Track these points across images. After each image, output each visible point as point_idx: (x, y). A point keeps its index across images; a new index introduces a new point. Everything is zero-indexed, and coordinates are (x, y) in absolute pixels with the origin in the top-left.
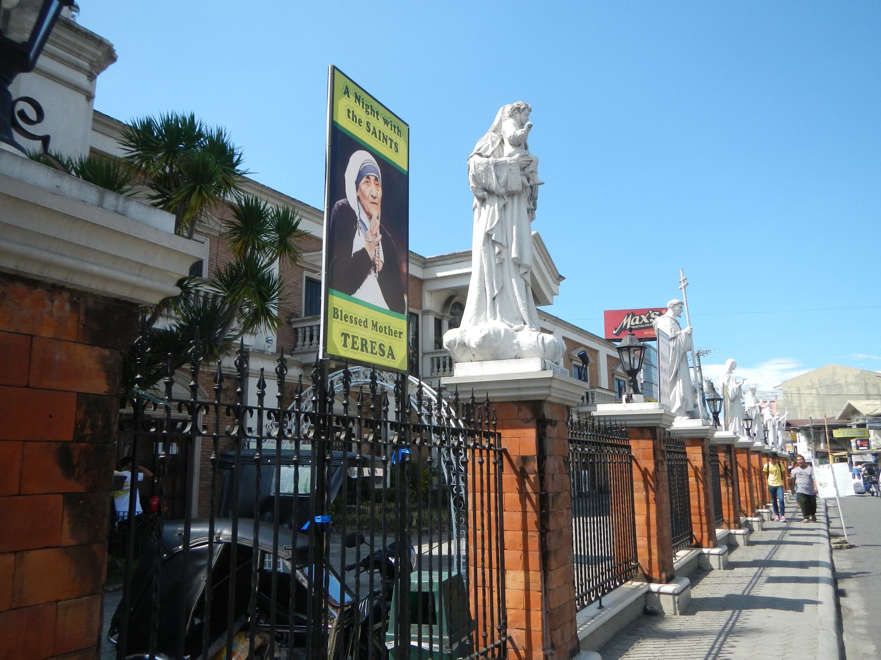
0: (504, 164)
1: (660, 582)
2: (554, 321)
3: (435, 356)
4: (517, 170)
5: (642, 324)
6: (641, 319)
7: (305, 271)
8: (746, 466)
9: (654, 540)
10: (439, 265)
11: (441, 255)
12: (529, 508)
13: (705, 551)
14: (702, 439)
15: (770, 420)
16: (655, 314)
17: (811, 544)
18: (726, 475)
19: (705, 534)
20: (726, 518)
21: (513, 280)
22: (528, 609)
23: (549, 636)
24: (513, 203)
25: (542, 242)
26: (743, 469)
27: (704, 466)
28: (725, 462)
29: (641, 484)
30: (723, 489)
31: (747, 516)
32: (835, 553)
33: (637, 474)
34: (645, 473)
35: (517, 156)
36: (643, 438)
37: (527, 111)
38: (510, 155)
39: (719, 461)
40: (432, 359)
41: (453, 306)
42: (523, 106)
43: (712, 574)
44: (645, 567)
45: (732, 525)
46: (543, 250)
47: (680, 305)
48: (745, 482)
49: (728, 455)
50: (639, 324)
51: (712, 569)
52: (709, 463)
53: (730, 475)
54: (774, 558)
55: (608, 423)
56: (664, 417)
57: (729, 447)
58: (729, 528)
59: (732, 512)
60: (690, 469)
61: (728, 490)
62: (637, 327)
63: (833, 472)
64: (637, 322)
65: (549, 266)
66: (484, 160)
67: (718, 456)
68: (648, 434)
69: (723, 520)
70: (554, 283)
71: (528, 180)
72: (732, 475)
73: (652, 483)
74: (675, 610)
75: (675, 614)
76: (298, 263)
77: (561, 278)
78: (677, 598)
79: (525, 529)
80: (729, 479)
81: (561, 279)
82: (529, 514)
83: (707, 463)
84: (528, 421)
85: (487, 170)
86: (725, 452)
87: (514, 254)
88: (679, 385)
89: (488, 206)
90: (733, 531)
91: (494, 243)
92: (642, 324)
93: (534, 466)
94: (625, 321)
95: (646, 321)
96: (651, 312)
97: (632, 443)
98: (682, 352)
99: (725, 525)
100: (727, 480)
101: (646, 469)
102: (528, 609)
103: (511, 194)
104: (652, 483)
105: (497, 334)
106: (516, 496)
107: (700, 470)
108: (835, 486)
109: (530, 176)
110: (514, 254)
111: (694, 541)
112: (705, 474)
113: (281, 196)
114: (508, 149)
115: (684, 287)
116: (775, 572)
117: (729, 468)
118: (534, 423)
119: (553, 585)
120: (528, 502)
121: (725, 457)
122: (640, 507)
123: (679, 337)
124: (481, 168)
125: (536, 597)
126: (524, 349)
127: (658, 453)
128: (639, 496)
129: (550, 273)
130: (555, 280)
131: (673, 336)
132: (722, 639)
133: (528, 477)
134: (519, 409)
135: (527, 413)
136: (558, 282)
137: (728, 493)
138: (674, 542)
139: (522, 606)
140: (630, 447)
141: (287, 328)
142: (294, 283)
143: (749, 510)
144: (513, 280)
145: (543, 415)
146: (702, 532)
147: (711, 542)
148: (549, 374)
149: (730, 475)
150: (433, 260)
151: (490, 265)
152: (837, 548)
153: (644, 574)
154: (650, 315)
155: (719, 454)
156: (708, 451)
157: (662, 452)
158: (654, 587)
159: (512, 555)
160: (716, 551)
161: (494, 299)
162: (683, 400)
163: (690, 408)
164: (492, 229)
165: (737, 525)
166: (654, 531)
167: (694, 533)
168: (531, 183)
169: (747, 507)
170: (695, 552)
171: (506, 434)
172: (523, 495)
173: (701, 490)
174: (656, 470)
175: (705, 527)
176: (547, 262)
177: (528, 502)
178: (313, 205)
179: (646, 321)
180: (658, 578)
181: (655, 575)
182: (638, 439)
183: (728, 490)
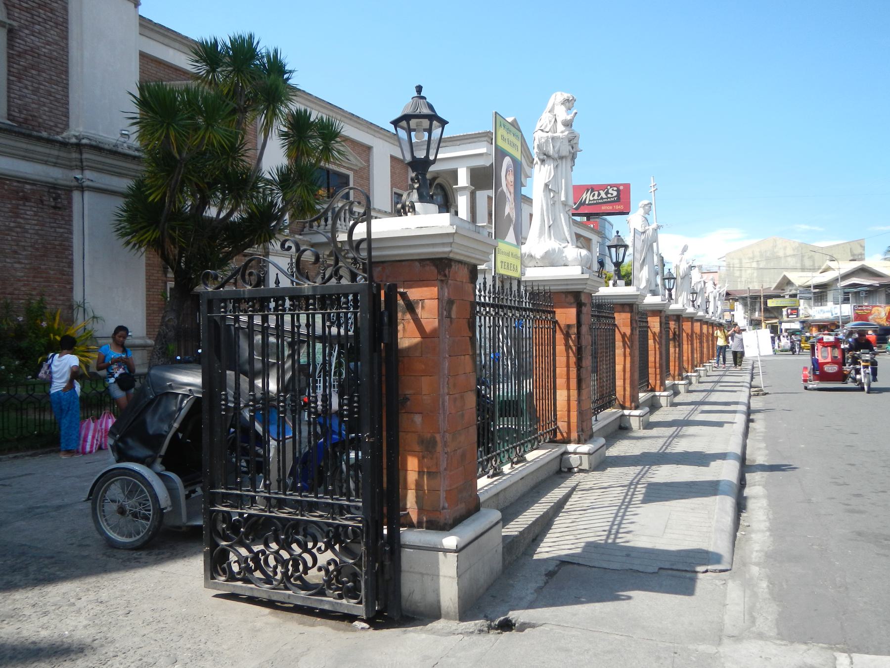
0: (558, 138)
1: (631, 409)
4: (566, 143)
5: (600, 199)
6: (599, 194)
8: (689, 332)
9: (628, 381)
12: (571, 354)
13: (657, 394)
14: (660, 311)
15: (712, 292)
16: (613, 190)
17: (735, 391)
18: (674, 339)
19: (658, 382)
20: (672, 372)
21: (562, 215)
22: (569, 411)
23: (580, 425)
24: (562, 163)
26: (688, 335)
27: (661, 332)
28: (674, 329)
29: (621, 344)
30: (672, 350)
31: (687, 372)
32: (752, 398)
33: (618, 337)
34: (624, 336)
35: (566, 133)
36: (624, 312)
37: (573, 101)
38: (562, 132)
39: (669, 328)
41: (435, 187)
42: (571, 98)
43: (662, 409)
44: (621, 399)
45: (677, 377)
47: (649, 205)
48: (688, 345)
50: (598, 200)
51: (662, 407)
52: (664, 329)
54: (707, 400)
55: (597, 301)
56: (639, 297)
57: (679, 317)
58: (674, 380)
59: (677, 368)
60: (650, 334)
61: (675, 351)
62: (595, 202)
64: (596, 197)
66: (545, 135)
67: (669, 324)
68: (628, 309)
69: (670, 374)
71: (573, 148)
73: (628, 343)
74: (640, 426)
75: (640, 429)
78: (641, 418)
79: (568, 366)
80: (676, 342)
82: (570, 358)
83: (663, 329)
84: (571, 304)
85: (547, 141)
86: (675, 321)
87: (563, 199)
88: (646, 268)
89: (546, 165)
90: (676, 382)
91: (550, 190)
92: (600, 199)
93: (575, 330)
94: (584, 196)
95: (604, 196)
96: (609, 187)
97: (616, 315)
98: (649, 244)
99: (671, 378)
101: (624, 333)
102: (569, 411)
103: (561, 158)
104: (628, 343)
105: (554, 250)
106: (563, 348)
109: (574, 146)
110: (563, 199)
111: (650, 387)
112: (660, 337)
114: (560, 127)
115: (654, 191)
116: (707, 408)
117: (677, 333)
118: (575, 305)
119: (583, 398)
120: (570, 351)
121: (675, 324)
122: (619, 359)
123: (647, 232)
124: (543, 140)
125: (574, 404)
126: (569, 260)
127: (634, 322)
128: (619, 351)
131: (643, 231)
132: (671, 439)
133: (571, 337)
134: (566, 297)
135: (571, 299)
137: (675, 353)
138: (640, 384)
139: (566, 409)
140: (615, 318)
144: (562, 215)
145: (581, 300)
146: (656, 380)
147: (662, 388)
148: (586, 276)
151: (547, 205)
153: (620, 404)
154: (608, 191)
155: (670, 323)
156: (663, 320)
157: (636, 321)
158: (626, 412)
159: (561, 381)
160: (665, 393)
161: (550, 227)
162: (648, 281)
163: (653, 287)
164: (549, 181)
165: (680, 377)
166: (628, 375)
167: (650, 381)
168: (574, 150)
170: (650, 394)
171: (558, 311)
172: (567, 347)
173: (657, 349)
174: (632, 334)
175: (658, 377)
177: (570, 351)
178: (314, 94)
179: (604, 196)
180: (629, 406)
181: (628, 404)
182: (620, 312)
183: (675, 351)
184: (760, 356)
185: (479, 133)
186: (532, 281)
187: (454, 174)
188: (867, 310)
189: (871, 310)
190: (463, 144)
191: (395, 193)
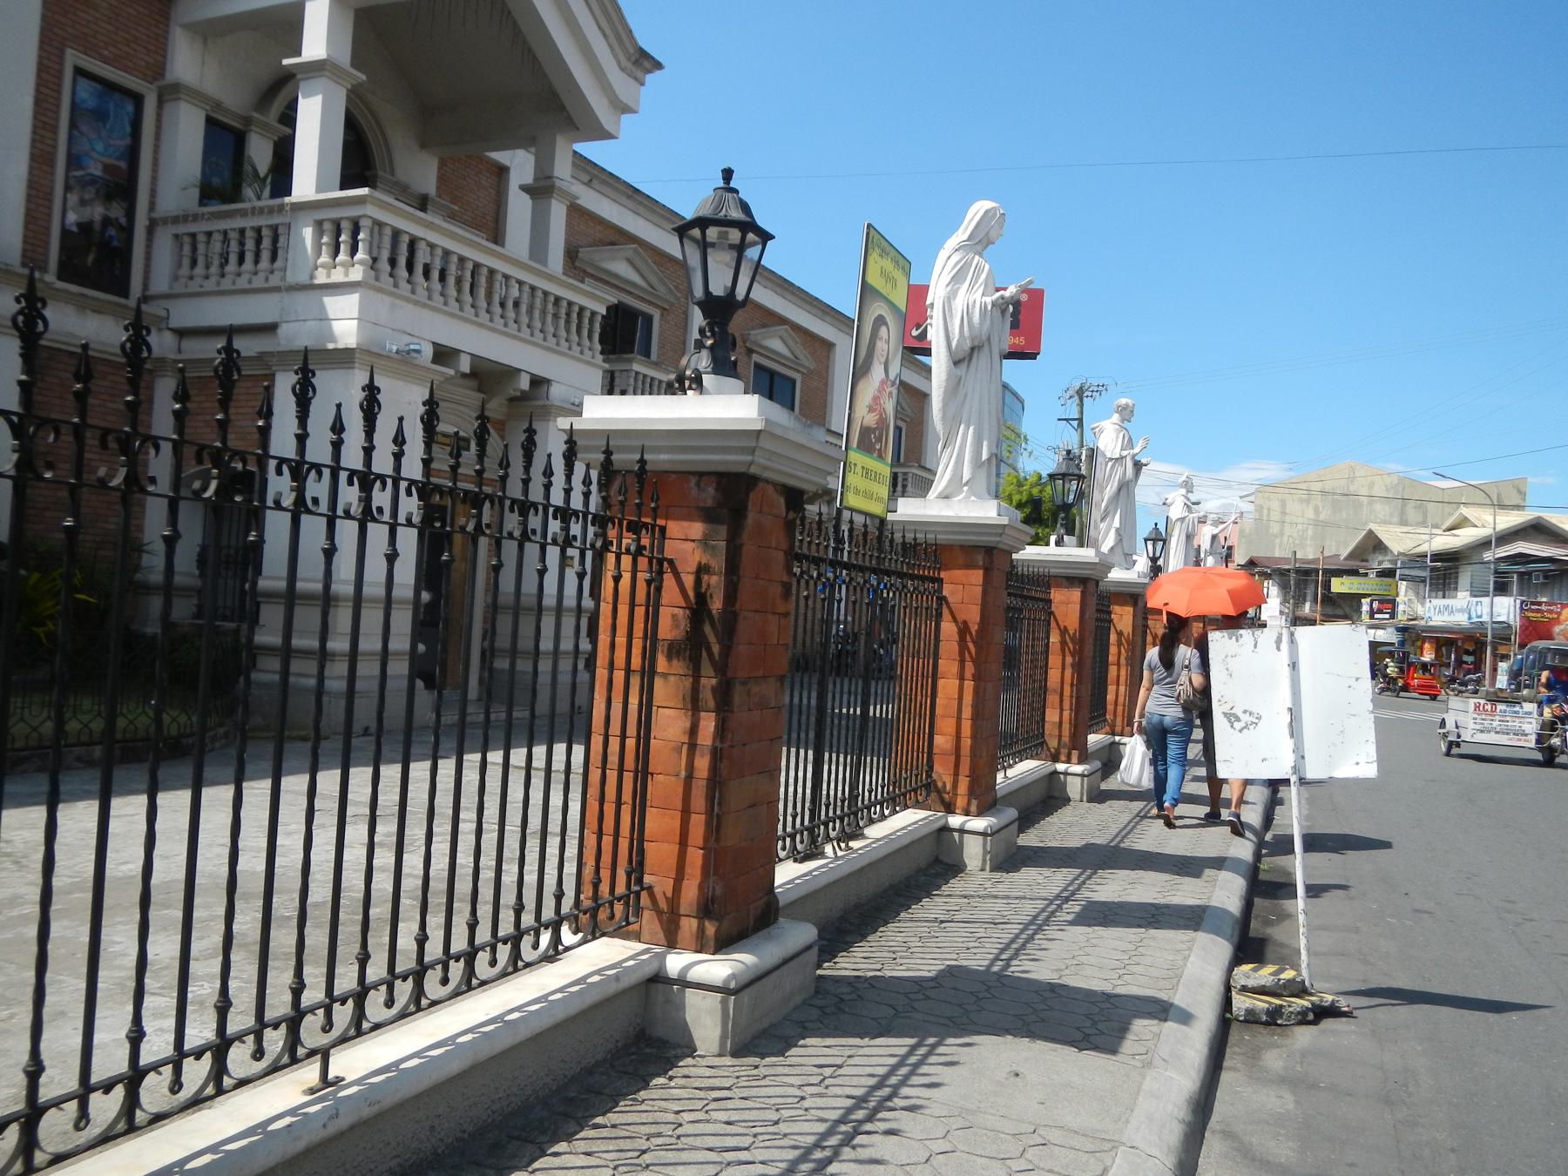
3: (182, 229)
15: (1182, 519)
26: (963, 630)
28: (701, 570)
30: (670, 724)
31: (950, 809)
40: (177, 236)
45: (689, 925)
48: (962, 678)
49: (723, 530)
53: (716, 649)
61: (693, 731)
63: (1294, 666)
70: (622, 70)
72: (727, 650)
77: (643, 62)
80: (707, 669)
81: (647, 64)
86: (708, 516)
100: (696, 676)
108: (1295, 729)
117: (716, 605)
121: (705, 542)
129: (605, 36)
130: (629, 65)
136: (639, 74)
137: (693, 747)
143: (963, 788)
149: (716, 649)
152: (1251, 1019)
155: (674, 528)
165: (710, 929)
169: (956, 774)
183: (693, 731)
184: (1302, 781)
186: (608, 435)
188: (1551, 612)
189: (1559, 614)
191: (79, 72)
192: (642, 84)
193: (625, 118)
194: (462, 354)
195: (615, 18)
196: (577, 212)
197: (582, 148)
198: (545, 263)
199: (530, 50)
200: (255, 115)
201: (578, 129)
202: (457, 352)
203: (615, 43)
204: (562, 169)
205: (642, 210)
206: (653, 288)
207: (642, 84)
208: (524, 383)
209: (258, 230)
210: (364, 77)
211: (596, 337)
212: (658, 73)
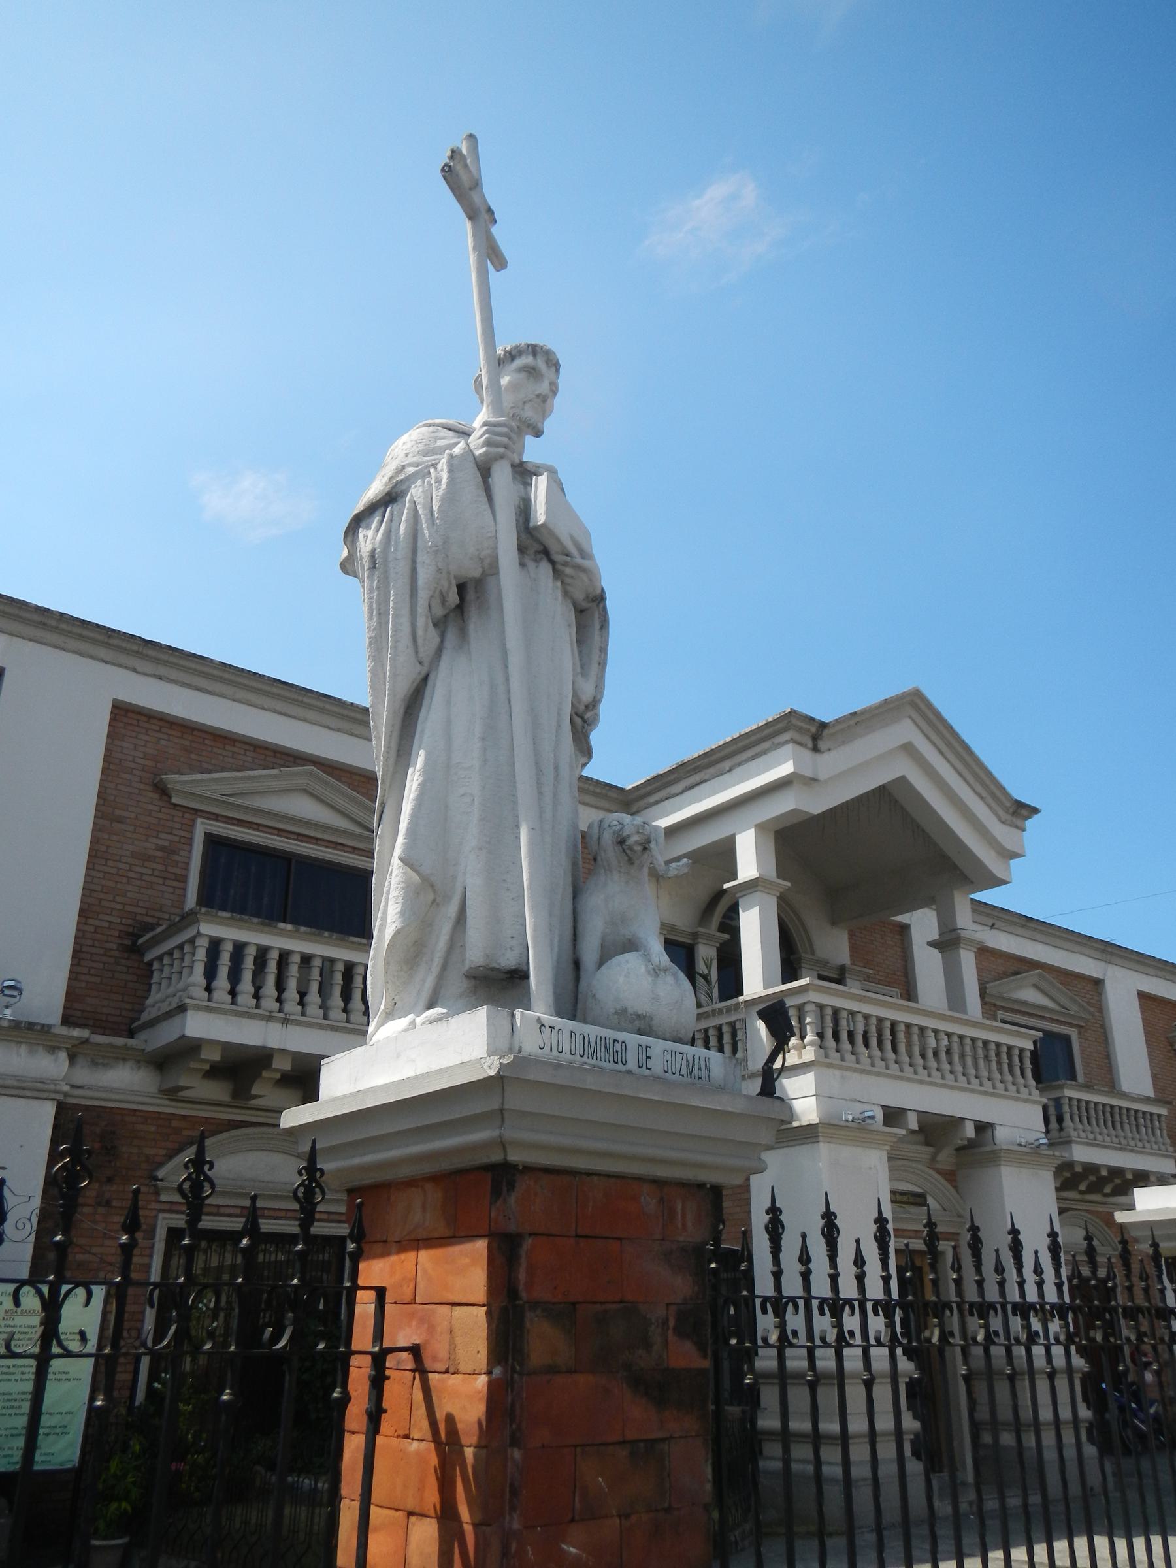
2: (1104, 951)
7: (199, 820)
10: (657, 803)
11: (655, 774)
25: (938, 715)
46: (948, 735)
65: (977, 777)
70: (1003, 823)
76: (174, 800)
77: (1021, 811)
81: (1024, 812)
107: (469, 1452)
113: (109, 637)
123: (416, 492)
129: (982, 798)
130: (1009, 817)
136: (1019, 822)
141: (123, 962)
142: (162, 848)
150: (643, 791)
176: (966, 765)
185: (768, 724)
187: (726, 853)
190: (739, 764)
192: (1024, 830)
193: (1013, 863)
194: (909, 1112)
195: (988, 782)
196: (984, 952)
197: (980, 896)
198: (964, 1011)
199: (918, 826)
200: (700, 929)
201: (972, 882)
202: (903, 1111)
203: (993, 804)
204: (964, 919)
205: (1038, 936)
206: (1066, 1009)
207: (1024, 830)
208: (970, 1131)
209: (719, 1029)
210: (789, 884)
211: (1029, 1073)
212: (1036, 816)
